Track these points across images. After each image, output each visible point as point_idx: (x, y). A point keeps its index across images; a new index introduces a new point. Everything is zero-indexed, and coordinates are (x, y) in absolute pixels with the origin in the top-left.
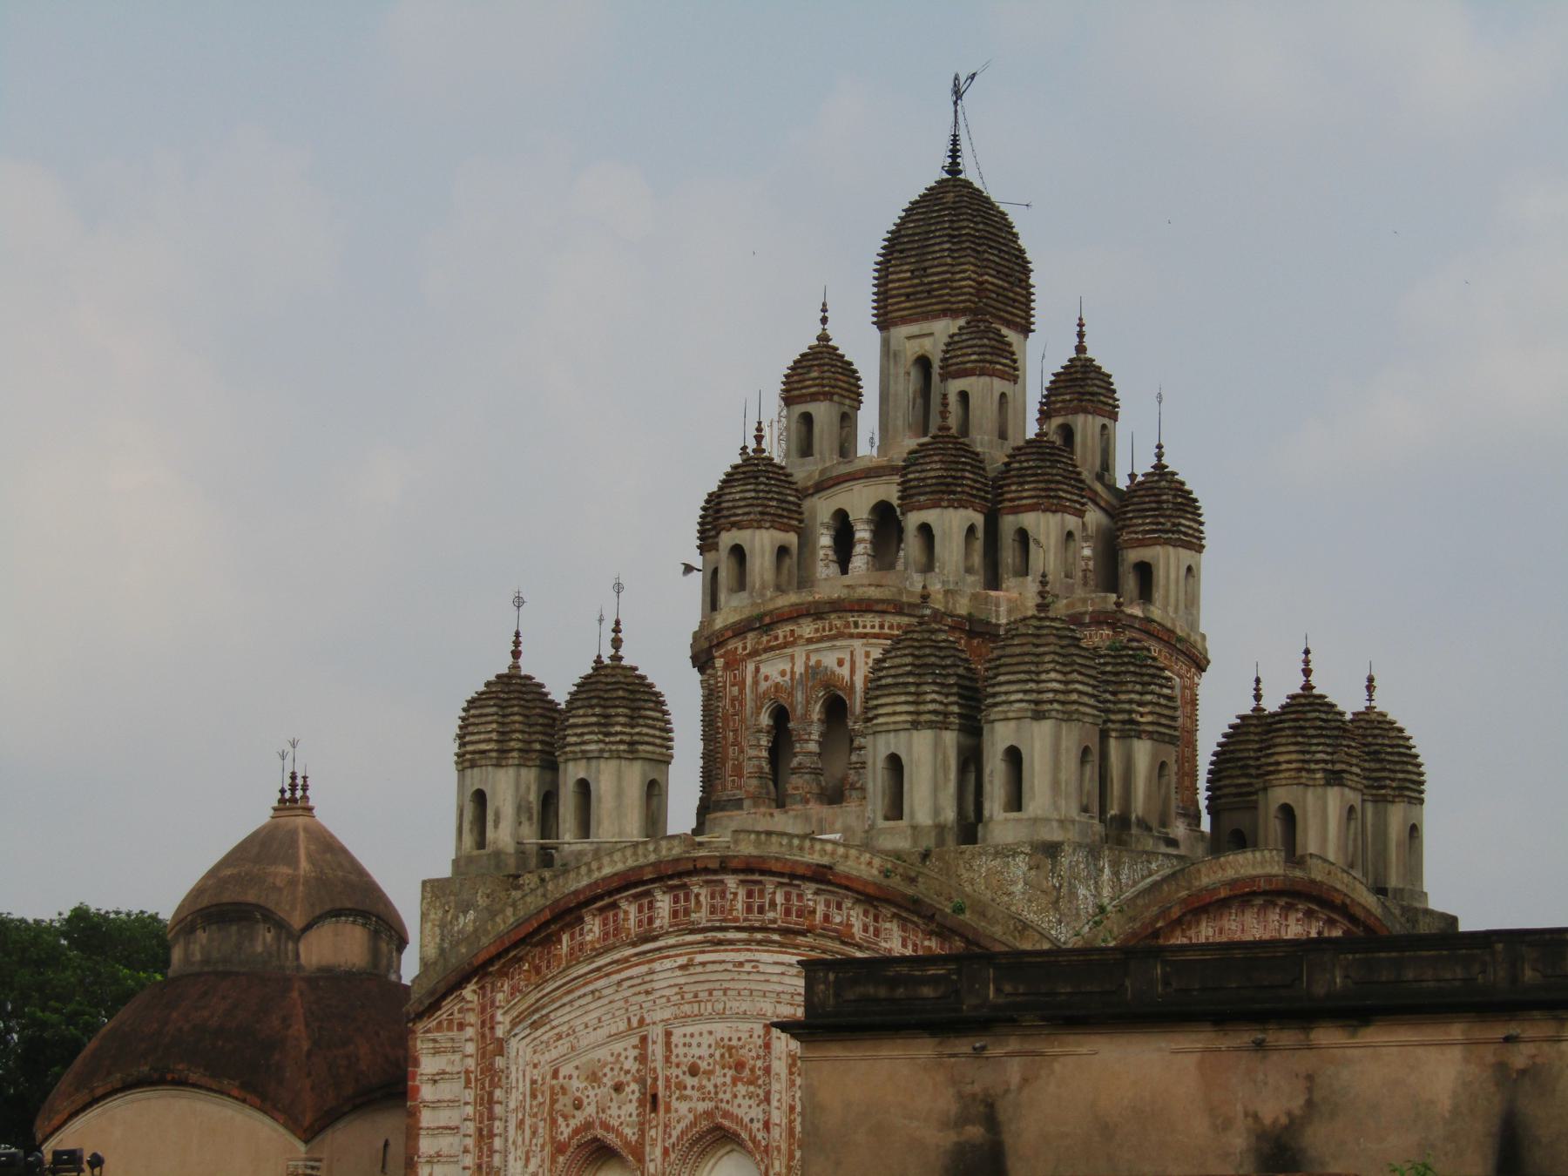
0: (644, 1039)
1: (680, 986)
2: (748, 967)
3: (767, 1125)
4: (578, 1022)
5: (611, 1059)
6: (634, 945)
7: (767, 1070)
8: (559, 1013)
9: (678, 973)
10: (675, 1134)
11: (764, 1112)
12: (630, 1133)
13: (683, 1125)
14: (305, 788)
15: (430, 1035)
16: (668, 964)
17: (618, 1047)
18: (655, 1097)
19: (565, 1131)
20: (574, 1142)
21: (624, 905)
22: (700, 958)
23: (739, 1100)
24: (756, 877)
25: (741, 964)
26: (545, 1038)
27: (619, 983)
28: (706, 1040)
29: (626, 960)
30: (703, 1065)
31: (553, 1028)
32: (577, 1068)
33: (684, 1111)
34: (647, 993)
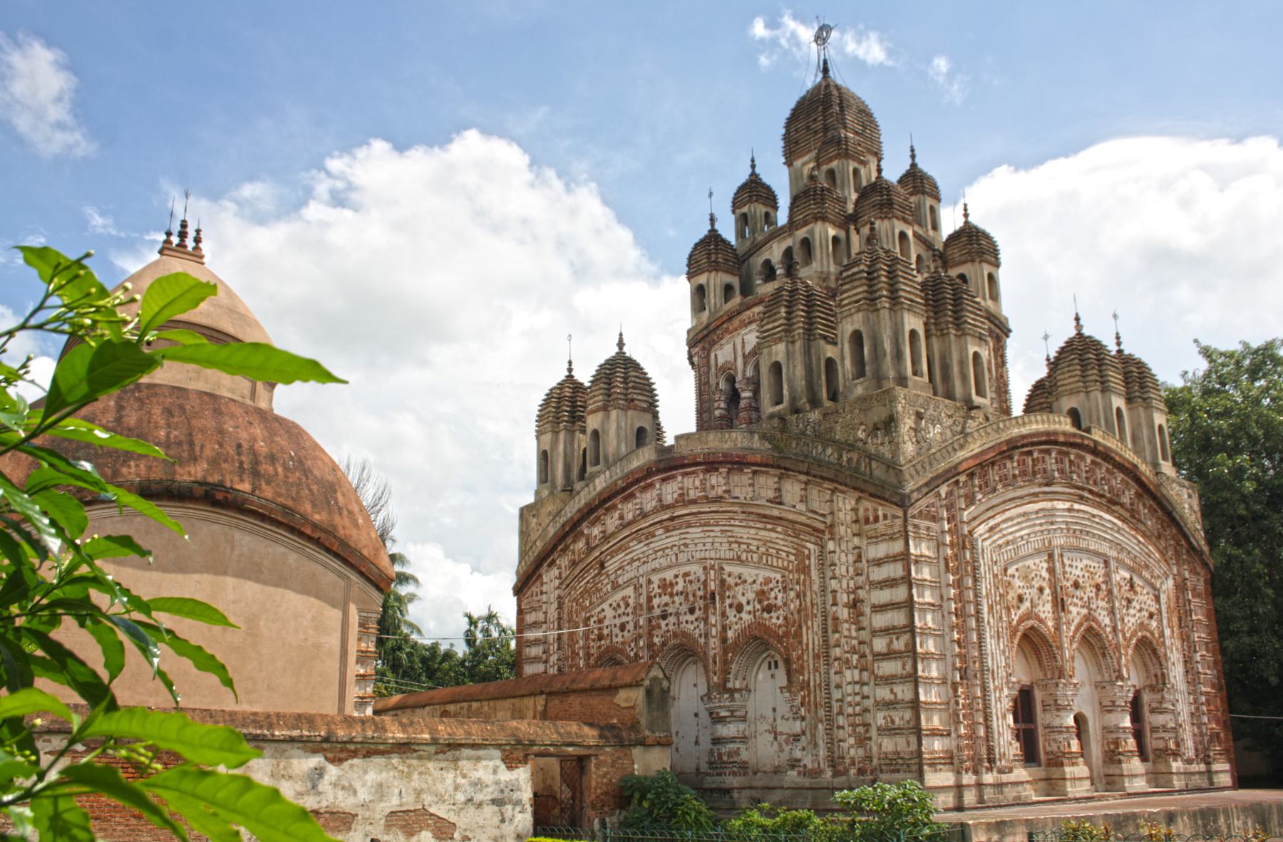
0: (1051, 556)
1: (1067, 523)
2: (1097, 520)
3: (1114, 629)
4: (1018, 535)
5: (1034, 567)
6: (1040, 485)
7: (1110, 592)
8: (1005, 526)
9: (1066, 514)
10: (1073, 628)
11: (1111, 621)
12: (1050, 624)
13: (1076, 622)
14: (197, 240)
15: (916, 521)
16: (1060, 505)
17: (1037, 561)
18: (1062, 600)
19: (1015, 619)
20: (1021, 628)
21: (1035, 455)
22: (1076, 506)
23: (1099, 611)
24: (1098, 460)
25: (1094, 516)
26: (1000, 542)
27: (1037, 512)
28: (1080, 565)
29: (1035, 495)
30: (1081, 581)
31: (1004, 536)
32: (1017, 570)
33: (1076, 612)
34: (1052, 523)
